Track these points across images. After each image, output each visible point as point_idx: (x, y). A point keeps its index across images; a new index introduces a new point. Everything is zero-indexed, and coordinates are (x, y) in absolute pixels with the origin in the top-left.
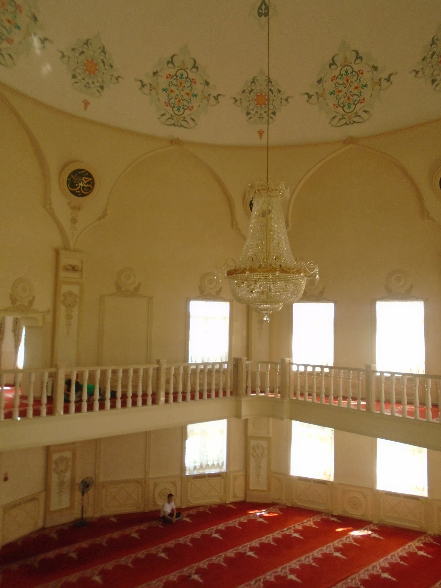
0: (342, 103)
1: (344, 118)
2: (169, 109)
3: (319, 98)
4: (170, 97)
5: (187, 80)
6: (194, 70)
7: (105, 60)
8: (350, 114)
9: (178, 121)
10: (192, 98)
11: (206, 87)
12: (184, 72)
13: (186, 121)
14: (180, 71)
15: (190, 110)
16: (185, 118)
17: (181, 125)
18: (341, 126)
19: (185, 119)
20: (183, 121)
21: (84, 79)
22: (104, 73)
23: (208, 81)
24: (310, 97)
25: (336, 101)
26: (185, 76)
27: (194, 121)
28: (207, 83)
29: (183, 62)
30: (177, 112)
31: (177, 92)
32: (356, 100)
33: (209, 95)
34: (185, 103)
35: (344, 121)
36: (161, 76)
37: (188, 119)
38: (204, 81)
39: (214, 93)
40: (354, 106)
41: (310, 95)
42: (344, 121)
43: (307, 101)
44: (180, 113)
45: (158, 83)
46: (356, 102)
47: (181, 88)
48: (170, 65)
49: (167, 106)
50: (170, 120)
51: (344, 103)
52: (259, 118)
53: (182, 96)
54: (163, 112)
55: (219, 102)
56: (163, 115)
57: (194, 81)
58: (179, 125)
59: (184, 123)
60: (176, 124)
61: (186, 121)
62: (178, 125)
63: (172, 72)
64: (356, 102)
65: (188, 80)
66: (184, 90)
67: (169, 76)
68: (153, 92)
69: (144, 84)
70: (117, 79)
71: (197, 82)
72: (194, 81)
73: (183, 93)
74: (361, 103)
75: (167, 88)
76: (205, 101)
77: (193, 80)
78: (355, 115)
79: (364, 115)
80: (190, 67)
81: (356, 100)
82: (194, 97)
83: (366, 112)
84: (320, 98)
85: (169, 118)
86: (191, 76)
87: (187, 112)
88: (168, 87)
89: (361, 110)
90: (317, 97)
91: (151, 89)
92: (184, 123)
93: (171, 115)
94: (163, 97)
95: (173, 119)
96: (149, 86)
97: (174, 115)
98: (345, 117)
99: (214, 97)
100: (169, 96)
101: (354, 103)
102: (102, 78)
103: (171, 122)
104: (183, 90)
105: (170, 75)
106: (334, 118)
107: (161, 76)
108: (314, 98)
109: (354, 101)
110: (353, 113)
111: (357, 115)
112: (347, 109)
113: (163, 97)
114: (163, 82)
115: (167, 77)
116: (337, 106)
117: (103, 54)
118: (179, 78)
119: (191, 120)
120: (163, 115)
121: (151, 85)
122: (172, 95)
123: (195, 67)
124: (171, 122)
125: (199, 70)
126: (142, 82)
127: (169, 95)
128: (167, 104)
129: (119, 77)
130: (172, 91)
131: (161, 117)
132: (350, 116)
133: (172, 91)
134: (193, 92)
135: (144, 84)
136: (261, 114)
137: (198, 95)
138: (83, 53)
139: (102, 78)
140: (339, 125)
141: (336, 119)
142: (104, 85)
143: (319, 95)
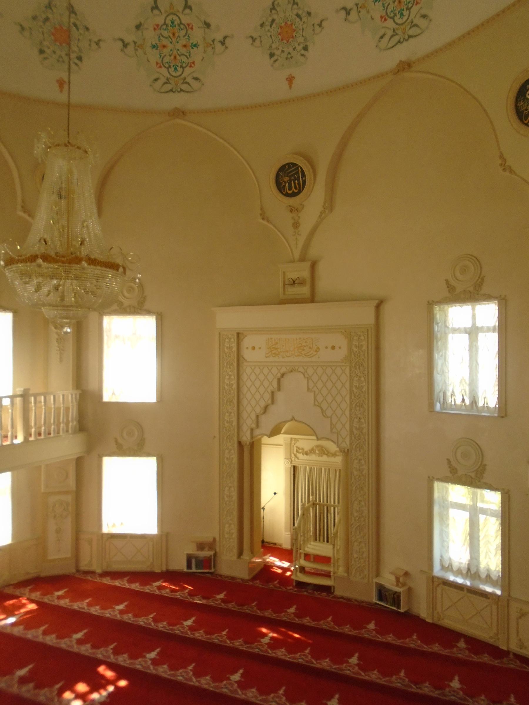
0: (392, 12)
1: (397, 34)
2: (164, 71)
3: (360, 12)
4: (163, 55)
5: (180, 27)
6: (188, 11)
7: (78, 23)
8: (403, 27)
9: (176, 85)
10: (192, 50)
11: (207, 30)
12: (175, 18)
13: (187, 83)
14: (170, 17)
15: (191, 66)
16: (185, 79)
17: (181, 90)
18: (393, 47)
19: (185, 81)
20: (183, 83)
21: (54, 52)
22: (79, 40)
23: (208, 21)
24: (348, 13)
25: (383, 10)
26: (177, 22)
27: (198, 81)
28: (208, 25)
29: (171, 4)
30: (174, 74)
31: (170, 46)
32: (409, 2)
33: (213, 41)
34: (184, 59)
35: (396, 39)
36: (147, 29)
37: (189, 80)
38: (203, 22)
39: (219, 37)
40: (408, 11)
41: (348, 10)
42: (396, 39)
43: (345, 20)
44: (178, 74)
45: (144, 40)
46: (410, 5)
47: (175, 40)
48: (156, 12)
49: (160, 67)
50: (166, 85)
51: (393, 11)
52: (287, 58)
53: (178, 50)
54: (156, 76)
55: (227, 48)
56: (156, 80)
57: (189, 27)
58: (179, 90)
59: (184, 87)
60: (174, 90)
61: (187, 83)
62: (176, 90)
63: (160, 20)
64: (410, 5)
65: (182, 26)
66: (179, 42)
67: (157, 27)
68: (140, 51)
69: (126, 43)
70: (97, 44)
71: (194, 27)
72: (191, 26)
73: (179, 46)
74: (416, 4)
75: (156, 44)
76: (210, 49)
77: (188, 25)
78: (410, 25)
79: (423, 23)
80: (181, 9)
81: (409, 2)
82: (194, 48)
83: (424, 16)
84: (362, 10)
85: (165, 83)
86: (185, 20)
87: (188, 70)
88: (157, 42)
89: (418, 16)
90: (357, 10)
91: (136, 48)
92: (184, 87)
93: (167, 79)
94: (154, 56)
95: (170, 84)
96: (132, 44)
97: (171, 77)
98: (397, 32)
99: (220, 42)
100: (160, 53)
101: (408, 7)
102: (78, 46)
103: (168, 87)
104: (178, 42)
105: (158, 25)
106: (382, 37)
107: (147, 29)
108: (354, 15)
109: (406, 4)
110: (408, 23)
111: (412, 24)
112: (399, 18)
113: (154, 56)
114: (151, 36)
115: (155, 29)
116: (385, 17)
117: (73, 15)
118: (169, 27)
119: (193, 81)
120: (156, 80)
121: (135, 43)
122: (166, 51)
123: (187, 6)
124: (168, 87)
125: (193, 10)
126: (122, 40)
127: (161, 52)
128: (160, 65)
129: (99, 40)
130: (164, 46)
131: (154, 83)
132: (404, 29)
133: (164, 46)
134: (191, 41)
135: (126, 43)
136: (289, 53)
137: (199, 44)
138: (47, 19)
139: (78, 46)
140: (390, 45)
141: (386, 38)
142: (82, 55)
143: (359, 6)
